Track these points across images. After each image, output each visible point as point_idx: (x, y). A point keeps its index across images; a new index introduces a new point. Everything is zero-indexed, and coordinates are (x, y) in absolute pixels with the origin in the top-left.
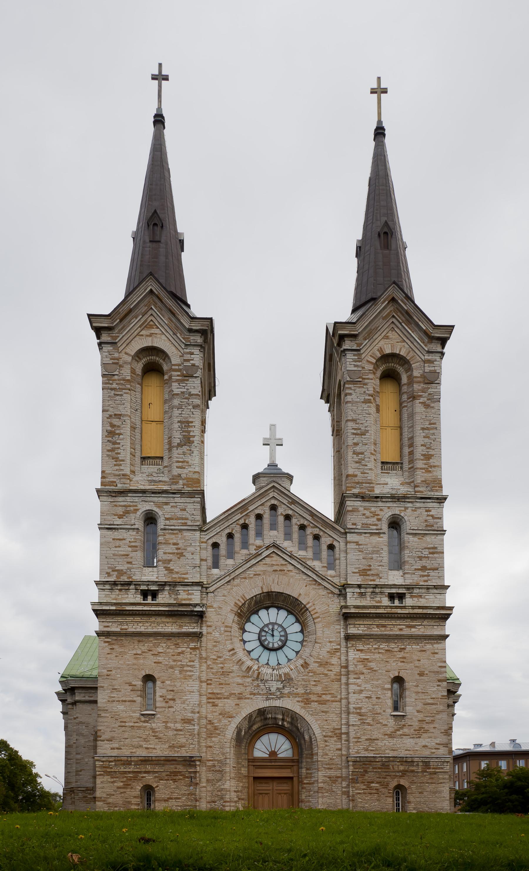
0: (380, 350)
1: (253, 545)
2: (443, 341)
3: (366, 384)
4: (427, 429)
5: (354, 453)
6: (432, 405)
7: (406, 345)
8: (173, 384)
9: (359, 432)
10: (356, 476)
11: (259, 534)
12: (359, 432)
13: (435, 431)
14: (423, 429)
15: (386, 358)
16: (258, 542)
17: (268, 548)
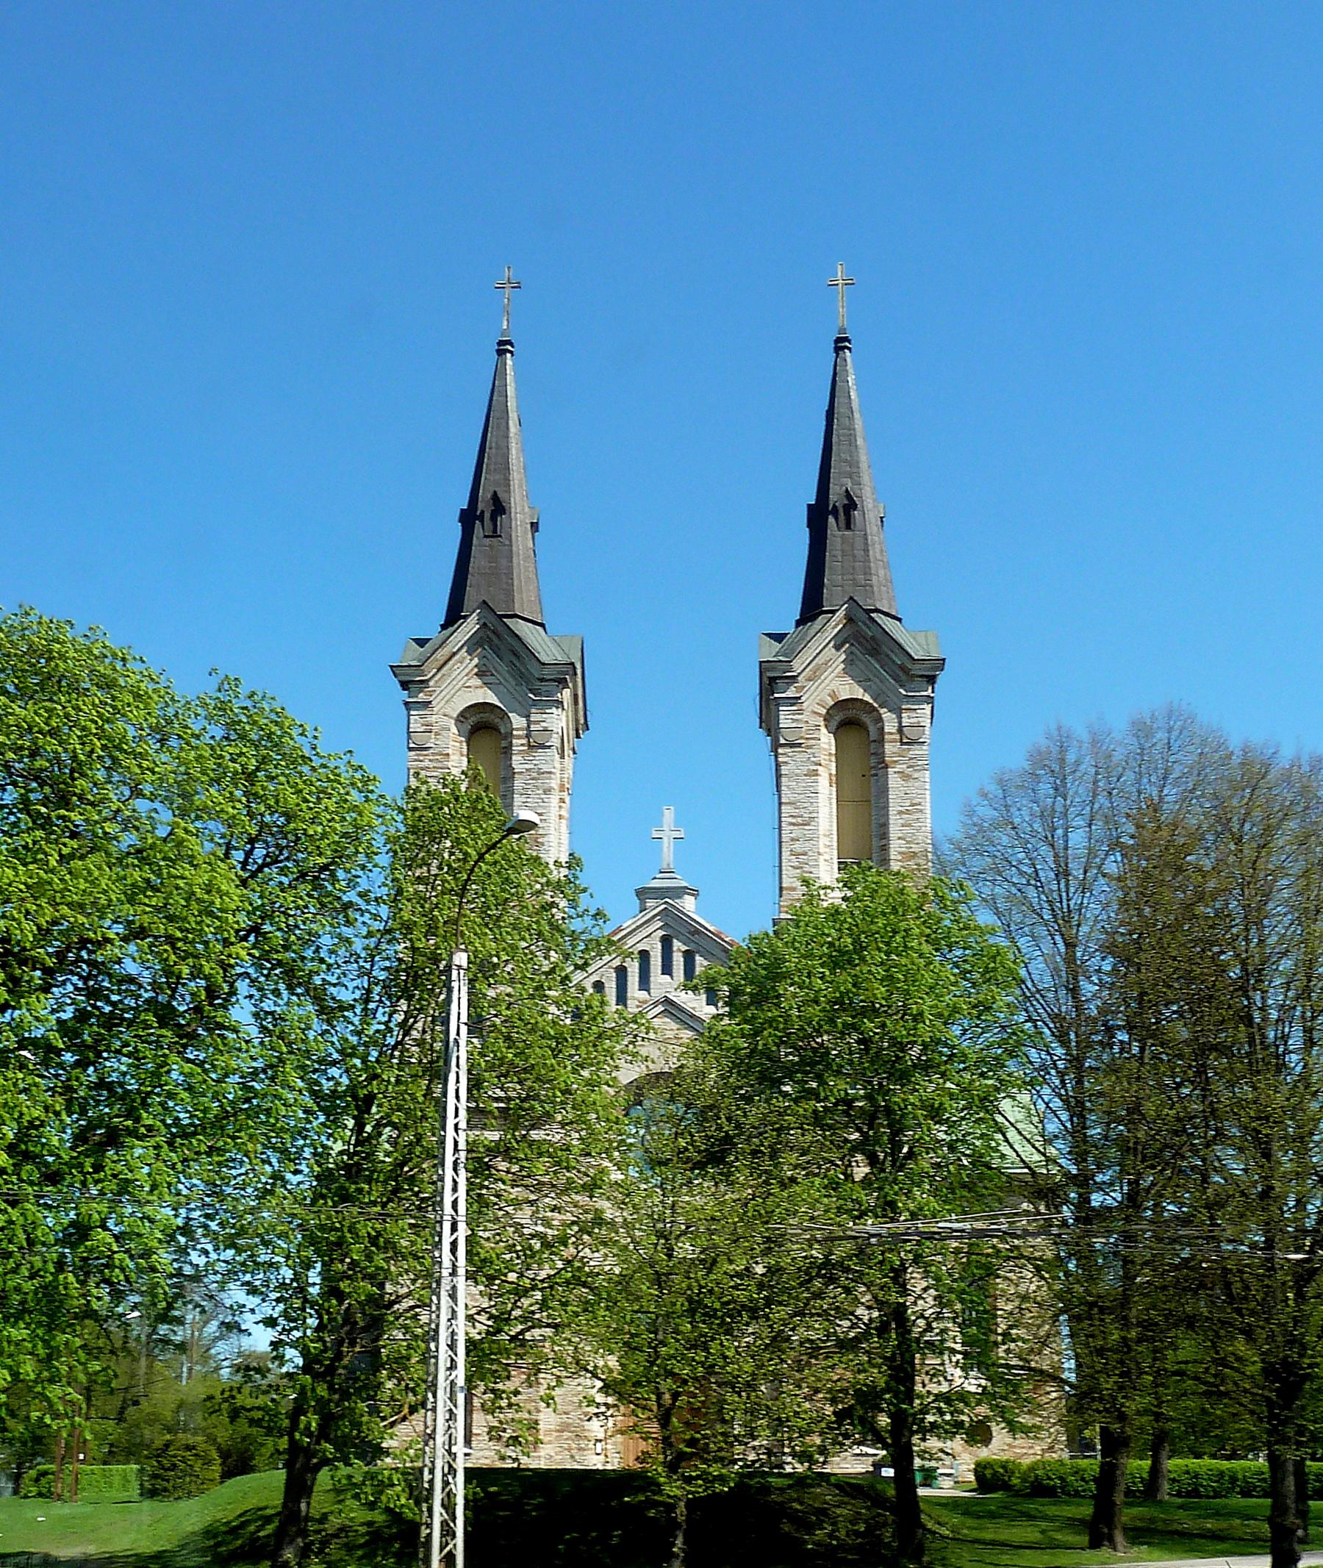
0: (833, 694)
1: (634, 999)
2: (931, 680)
3: (809, 747)
4: (908, 812)
5: (793, 853)
6: (916, 775)
7: (874, 687)
8: (514, 758)
9: (799, 820)
10: (794, 889)
11: (644, 983)
12: (799, 820)
13: (919, 815)
14: (900, 813)
15: (841, 705)
16: (643, 995)
17: (656, 1004)
